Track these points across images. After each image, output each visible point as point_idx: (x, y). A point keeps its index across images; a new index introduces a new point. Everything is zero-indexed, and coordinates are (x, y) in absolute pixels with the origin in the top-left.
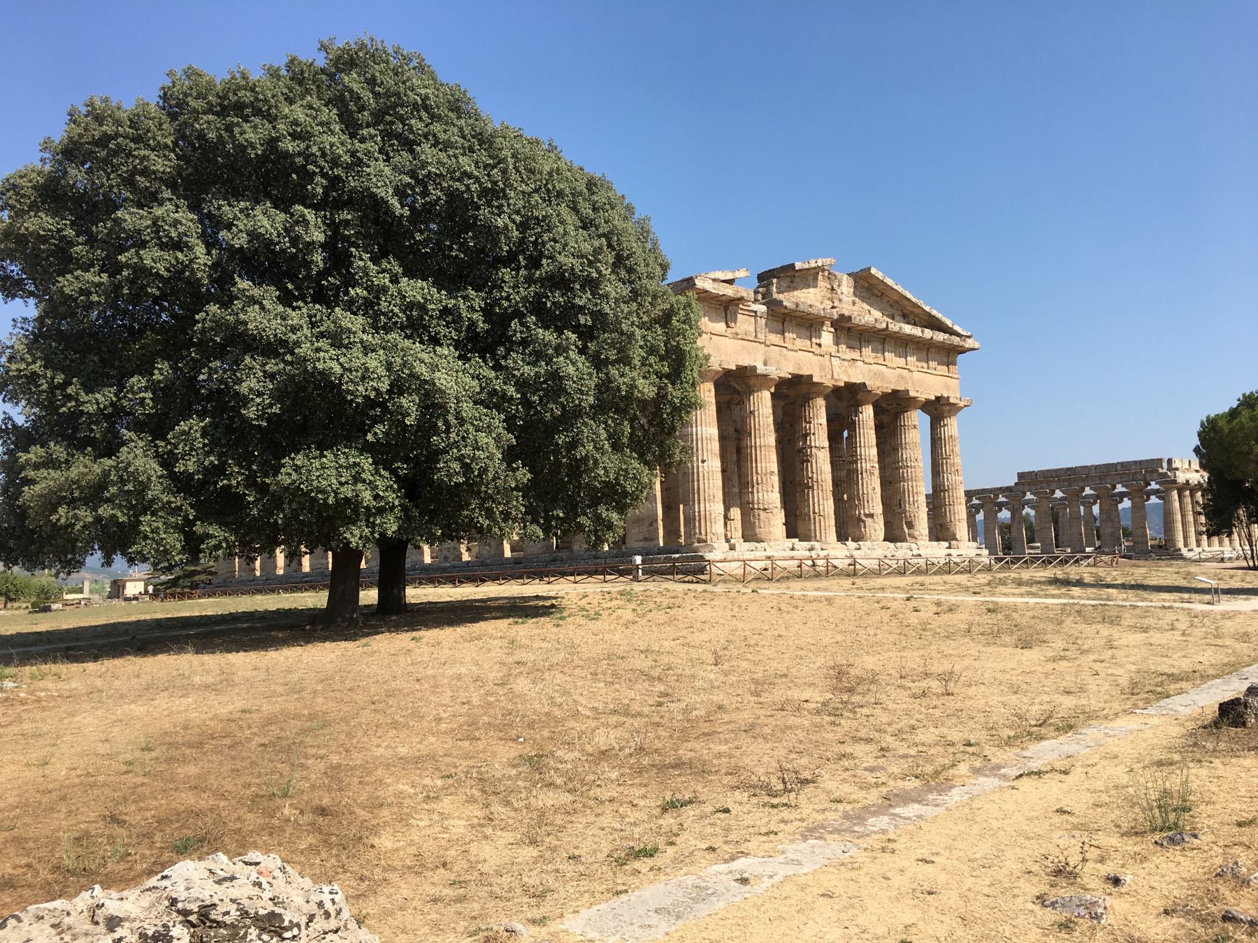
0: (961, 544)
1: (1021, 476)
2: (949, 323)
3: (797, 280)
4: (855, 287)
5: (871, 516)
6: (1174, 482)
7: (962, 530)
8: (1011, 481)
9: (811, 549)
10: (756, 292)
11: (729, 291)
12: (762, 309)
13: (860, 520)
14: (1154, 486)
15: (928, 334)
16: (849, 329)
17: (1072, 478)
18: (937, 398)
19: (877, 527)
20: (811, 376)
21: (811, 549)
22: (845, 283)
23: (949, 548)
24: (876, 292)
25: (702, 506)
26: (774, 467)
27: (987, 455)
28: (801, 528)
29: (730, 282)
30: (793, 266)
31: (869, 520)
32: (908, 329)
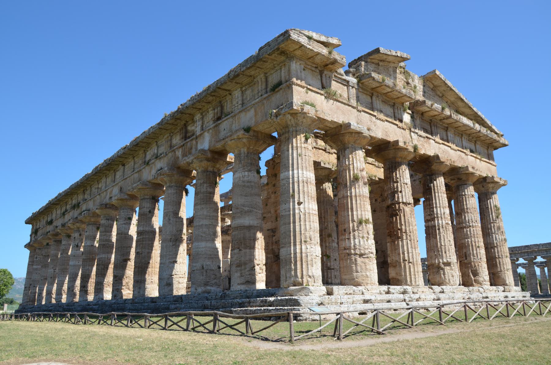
3: (381, 68)
5: (448, 264)
12: (353, 80)
13: (439, 268)
18: (485, 179)
19: (453, 273)
20: (397, 142)
21: (404, 292)
24: (438, 93)
25: (298, 247)
26: (368, 215)
28: (392, 273)
30: (377, 51)
31: (447, 269)
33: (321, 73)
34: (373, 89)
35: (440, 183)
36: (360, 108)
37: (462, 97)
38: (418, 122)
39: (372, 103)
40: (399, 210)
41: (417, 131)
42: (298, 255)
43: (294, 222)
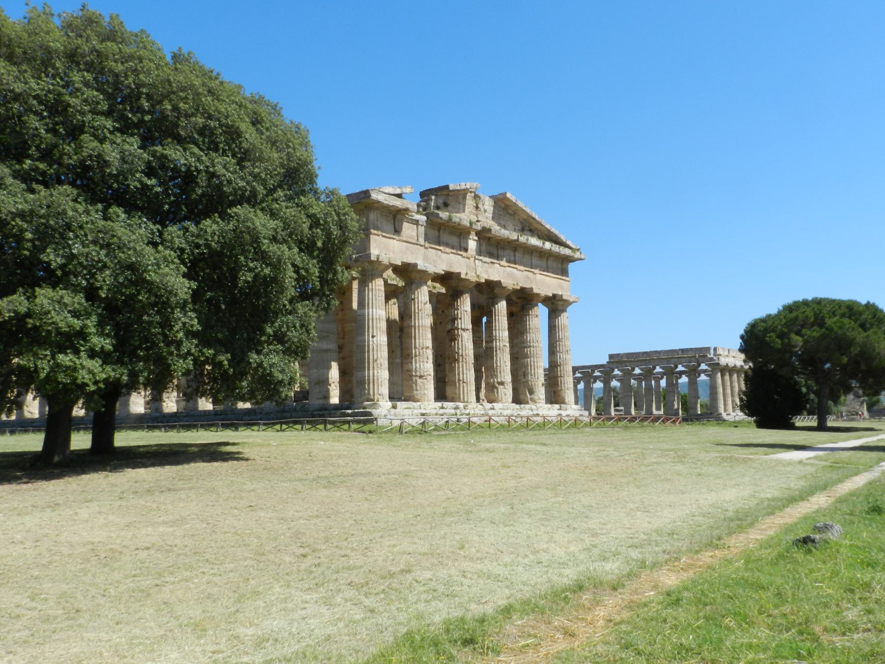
0: (568, 407)
1: (611, 356)
2: (563, 238)
4: (494, 207)
5: (502, 383)
6: (718, 364)
7: (569, 396)
8: (604, 360)
9: (456, 408)
10: (419, 206)
11: (398, 203)
12: (423, 218)
14: (703, 366)
15: (548, 245)
16: (489, 238)
17: (647, 359)
18: (554, 296)
19: (507, 392)
20: (459, 274)
21: (456, 408)
22: (487, 203)
23: (560, 409)
24: (510, 211)
25: (371, 372)
26: (429, 343)
27: (591, 338)
28: (449, 391)
29: (399, 196)
30: (447, 187)
31: (501, 387)
32: (534, 241)
33: (394, 217)
34: (440, 224)
35: (502, 307)
36: (427, 245)
37: (534, 216)
38: (484, 247)
39: (439, 237)
40: (458, 335)
41: (481, 258)
42: (371, 378)
43: (369, 352)
